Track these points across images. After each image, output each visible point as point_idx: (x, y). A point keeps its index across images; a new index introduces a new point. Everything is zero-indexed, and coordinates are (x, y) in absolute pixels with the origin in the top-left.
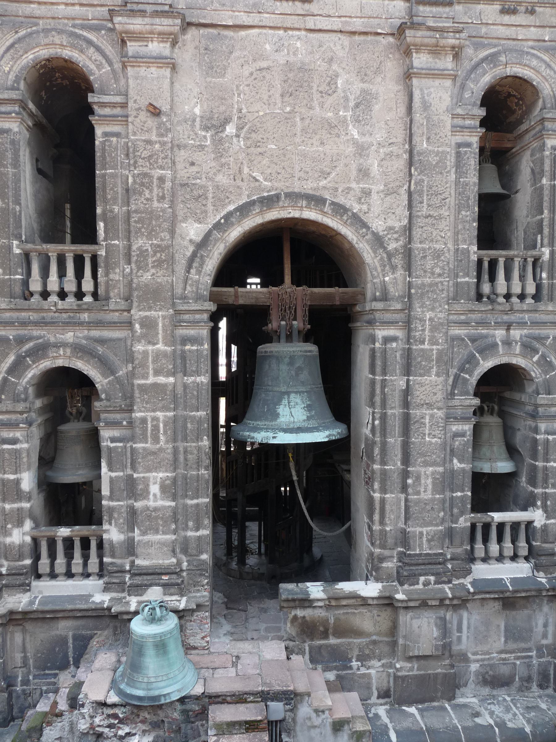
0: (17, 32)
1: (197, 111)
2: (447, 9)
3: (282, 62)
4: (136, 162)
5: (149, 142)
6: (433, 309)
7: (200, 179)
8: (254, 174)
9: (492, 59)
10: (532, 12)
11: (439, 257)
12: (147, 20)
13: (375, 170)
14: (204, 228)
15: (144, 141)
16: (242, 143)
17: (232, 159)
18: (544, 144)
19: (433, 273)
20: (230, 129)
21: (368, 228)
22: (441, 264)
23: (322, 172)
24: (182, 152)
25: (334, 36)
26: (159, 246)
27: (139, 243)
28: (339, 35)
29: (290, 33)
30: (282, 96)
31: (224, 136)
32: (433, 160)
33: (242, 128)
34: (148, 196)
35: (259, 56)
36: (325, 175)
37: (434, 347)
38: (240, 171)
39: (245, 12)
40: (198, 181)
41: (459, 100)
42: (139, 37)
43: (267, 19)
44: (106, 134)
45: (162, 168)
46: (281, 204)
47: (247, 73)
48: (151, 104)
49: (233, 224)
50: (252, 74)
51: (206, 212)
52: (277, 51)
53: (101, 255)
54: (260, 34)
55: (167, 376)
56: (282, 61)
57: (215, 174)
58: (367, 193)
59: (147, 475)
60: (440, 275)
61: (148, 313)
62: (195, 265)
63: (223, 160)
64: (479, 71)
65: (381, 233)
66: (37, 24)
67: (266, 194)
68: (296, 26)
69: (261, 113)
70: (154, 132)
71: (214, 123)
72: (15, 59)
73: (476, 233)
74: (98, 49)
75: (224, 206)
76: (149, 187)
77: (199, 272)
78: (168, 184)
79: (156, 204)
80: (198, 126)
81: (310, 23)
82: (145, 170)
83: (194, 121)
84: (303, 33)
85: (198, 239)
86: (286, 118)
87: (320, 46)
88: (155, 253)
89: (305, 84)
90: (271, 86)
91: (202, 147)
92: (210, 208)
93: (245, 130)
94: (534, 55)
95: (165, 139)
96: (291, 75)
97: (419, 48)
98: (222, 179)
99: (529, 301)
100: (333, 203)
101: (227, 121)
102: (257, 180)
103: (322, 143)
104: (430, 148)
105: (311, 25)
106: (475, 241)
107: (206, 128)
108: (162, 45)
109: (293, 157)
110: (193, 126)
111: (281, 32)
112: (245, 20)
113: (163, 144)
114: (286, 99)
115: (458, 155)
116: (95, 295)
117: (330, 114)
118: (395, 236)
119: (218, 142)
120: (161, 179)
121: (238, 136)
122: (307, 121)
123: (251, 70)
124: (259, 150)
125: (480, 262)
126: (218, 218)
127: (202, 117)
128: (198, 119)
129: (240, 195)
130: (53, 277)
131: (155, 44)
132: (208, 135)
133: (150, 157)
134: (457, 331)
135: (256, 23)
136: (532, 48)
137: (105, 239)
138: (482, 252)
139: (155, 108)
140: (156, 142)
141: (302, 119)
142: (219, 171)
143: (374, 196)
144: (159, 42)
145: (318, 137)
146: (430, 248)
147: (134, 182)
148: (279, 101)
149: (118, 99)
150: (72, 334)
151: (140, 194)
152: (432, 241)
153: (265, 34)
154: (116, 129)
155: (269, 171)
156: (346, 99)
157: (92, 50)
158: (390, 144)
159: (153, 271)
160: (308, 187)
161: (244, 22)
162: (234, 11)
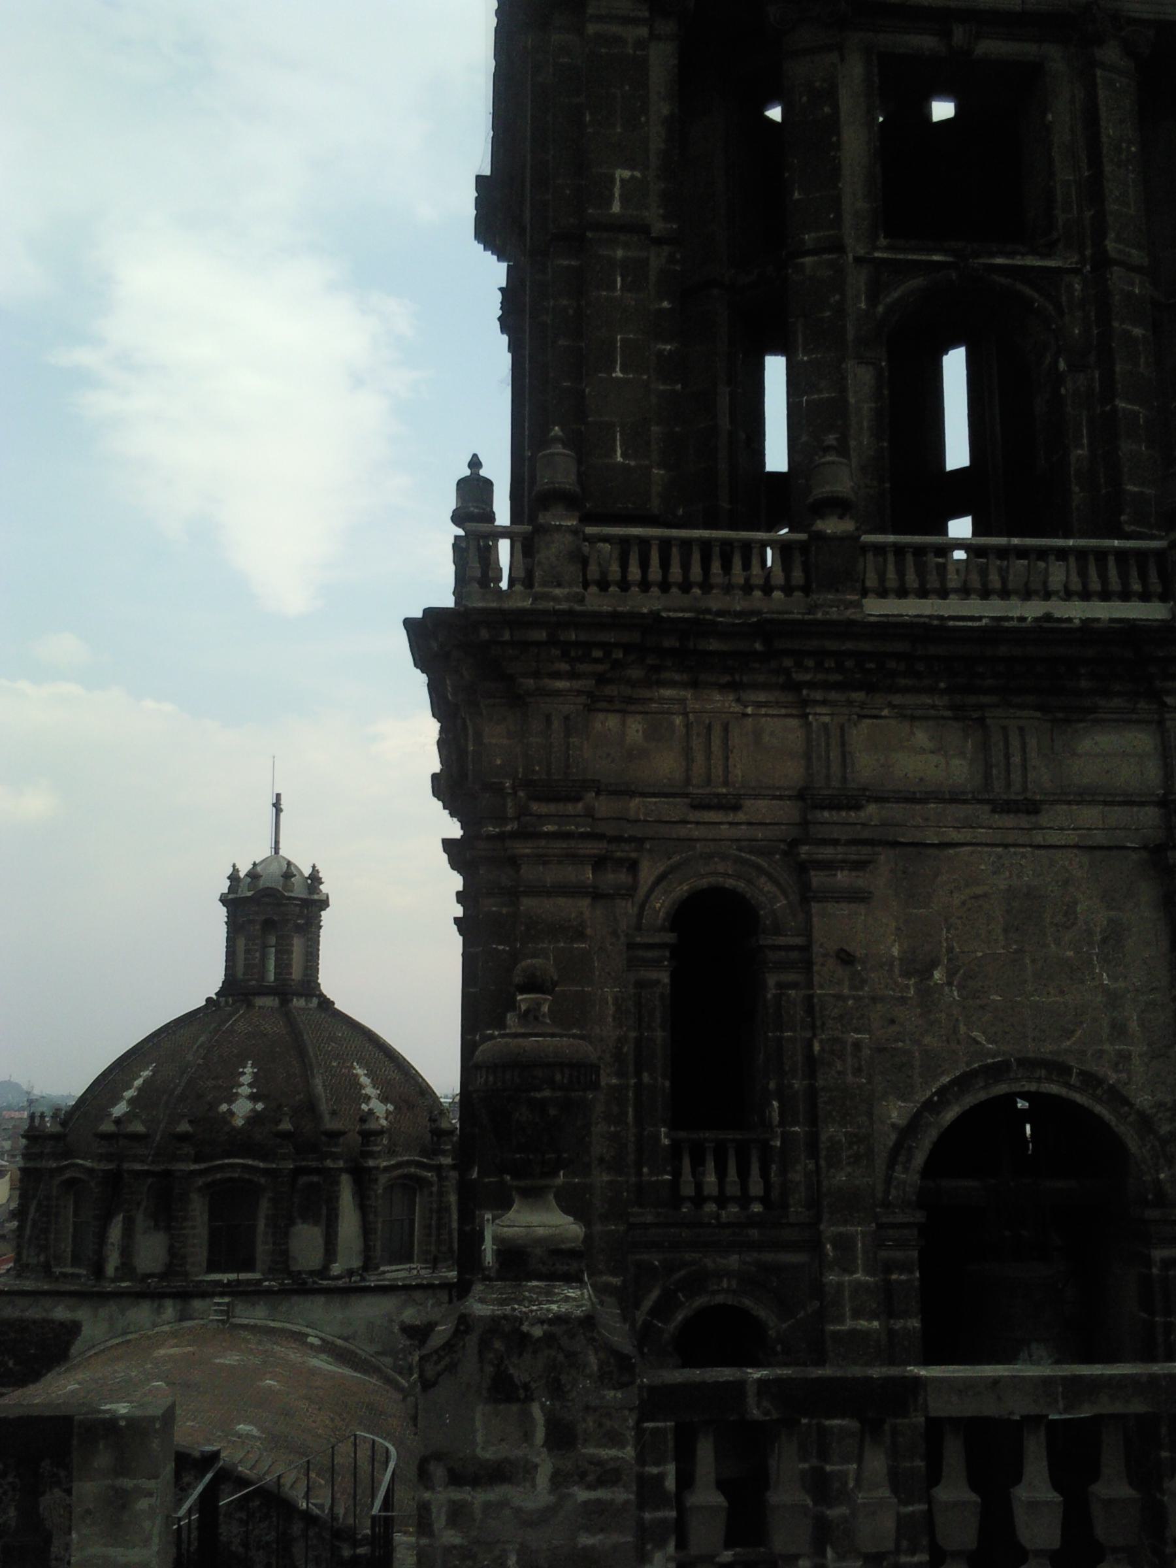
0: (670, 858)
1: (895, 951)
3: (1002, 887)
4: (823, 1024)
5: (839, 997)
12: (840, 849)
13: (1134, 1025)
14: (912, 1107)
15: (834, 996)
16: (955, 993)
17: (943, 1016)
21: (1131, 1105)
24: (879, 1006)
27: (830, 1131)
28: (1075, 851)
29: (1012, 850)
30: (1005, 931)
31: (932, 984)
34: (839, 1068)
36: (1069, 1033)
38: (955, 1030)
39: (954, 827)
40: (900, 1044)
42: (829, 866)
44: (780, 985)
45: (857, 1031)
46: (1012, 1075)
48: (842, 950)
50: (964, 903)
52: (994, 873)
53: (776, 1146)
54: (972, 852)
55: (869, 1320)
58: (1125, 1057)
59: (845, 1467)
61: (842, 1229)
62: (901, 1159)
65: (1149, 1112)
67: (990, 1061)
68: (1020, 841)
69: (979, 954)
74: (770, 877)
77: (906, 1170)
78: (866, 1052)
79: (850, 1079)
80: (897, 971)
81: (1039, 839)
83: (892, 965)
85: (902, 1122)
91: (903, 1000)
95: (861, 993)
100: (1082, 1073)
101: (934, 964)
102: (978, 1043)
103: (1062, 992)
107: (907, 974)
108: (854, 874)
111: (999, 850)
112: (955, 836)
113: (857, 999)
116: (765, 1200)
118: (1168, 1114)
120: (857, 1045)
121: (950, 984)
123: (963, 897)
126: (928, 1094)
127: (901, 959)
128: (897, 963)
132: (912, 982)
135: (969, 838)
137: (782, 1123)
139: (848, 954)
141: (1033, 961)
143: (1136, 1061)
144: (850, 870)
147: (822, 1050)
149: (798, 941)
150: (736, 1257)
153: (980, 852)
154: (791, 977)
157: (763, 879)
158: (1152, 990)
159: (849, 1169)
160: (1048, 1049)
161: (953, 839)
162: (940, 827)
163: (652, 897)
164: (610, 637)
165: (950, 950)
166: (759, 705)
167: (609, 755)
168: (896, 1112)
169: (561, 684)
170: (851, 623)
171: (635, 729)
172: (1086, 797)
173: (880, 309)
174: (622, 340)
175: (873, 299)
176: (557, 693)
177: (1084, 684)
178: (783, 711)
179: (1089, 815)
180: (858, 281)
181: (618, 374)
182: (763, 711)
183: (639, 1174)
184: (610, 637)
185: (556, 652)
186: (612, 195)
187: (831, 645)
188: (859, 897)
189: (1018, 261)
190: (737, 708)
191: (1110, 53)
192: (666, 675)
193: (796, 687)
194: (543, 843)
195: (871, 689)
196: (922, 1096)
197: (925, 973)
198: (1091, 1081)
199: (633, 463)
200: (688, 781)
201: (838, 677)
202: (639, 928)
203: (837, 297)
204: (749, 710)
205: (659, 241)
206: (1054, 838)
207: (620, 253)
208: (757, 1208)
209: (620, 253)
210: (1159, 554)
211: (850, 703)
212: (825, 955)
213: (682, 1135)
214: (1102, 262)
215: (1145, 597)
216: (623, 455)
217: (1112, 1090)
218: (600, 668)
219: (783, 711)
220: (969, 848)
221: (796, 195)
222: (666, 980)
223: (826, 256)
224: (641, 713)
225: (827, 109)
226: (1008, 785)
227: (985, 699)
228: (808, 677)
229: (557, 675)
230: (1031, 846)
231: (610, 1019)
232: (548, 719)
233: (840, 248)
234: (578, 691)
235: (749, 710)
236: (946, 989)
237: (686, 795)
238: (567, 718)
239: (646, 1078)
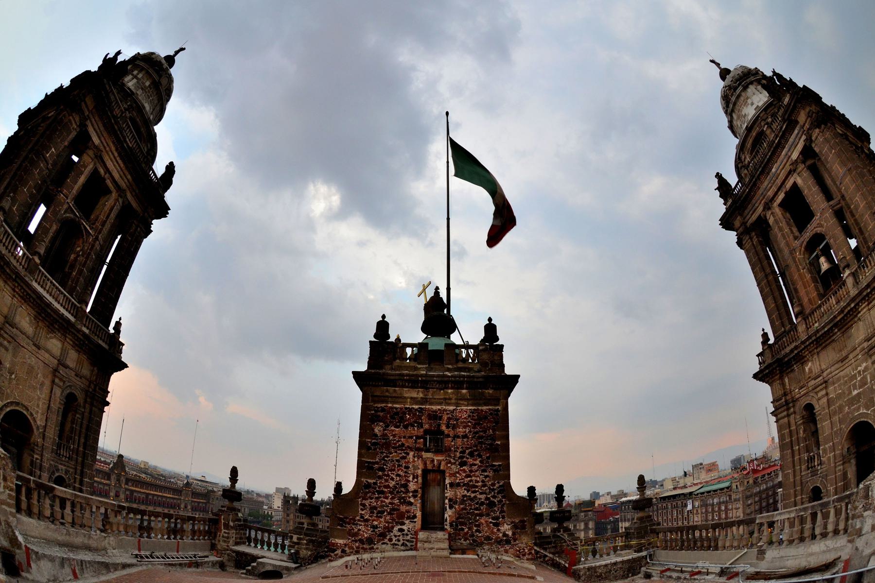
1: (8, 366)
10: (81, 378)
20: (13, 376)
35: (25, 358)
43: (29, 348)
97: (57, 377)
101: (13, 373)
107: (9, 373)
112: (25, 346)
119: (10, 379)
170: (28, 283)
172: (47, 351)
175: (64, 214)
177: (56, 327)
179: (47, 355)
180: (65, 206)
187: (24, 287)
188: (7, 349)
189: (87, 226)
190: (3, 287)
191: (121, 200)
193: (14, 291)
195: (25, 301)
197: (11, 374)
198: (32, 415)
205: (47, 168)
206: (40, 357)
209: (42, 165)
210: (78, 307)
211: (21, 302)
214: (97, 238)
217: (34, 418)
220: (26, 350)
226: (37, 340)
227: (40, 318)
228: (17, 290)
233: (67, 198)
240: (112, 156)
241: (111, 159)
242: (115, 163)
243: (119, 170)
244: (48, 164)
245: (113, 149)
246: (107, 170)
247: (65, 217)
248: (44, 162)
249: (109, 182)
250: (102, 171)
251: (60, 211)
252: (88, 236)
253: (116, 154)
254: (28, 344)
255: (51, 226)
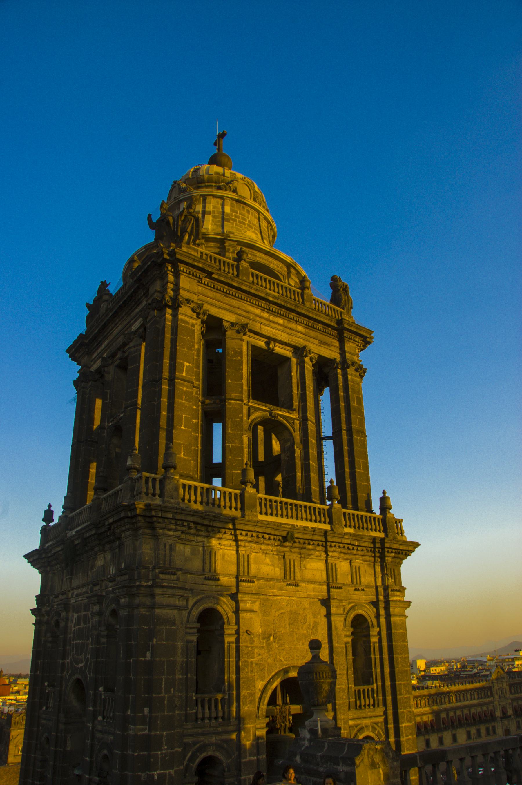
1: (260, 631)
2: (340, 590)
4: (242, 655)
5: (247, 647)
6: (344, 714)
7: (262, 661)
8: (281, 658)
9: (352, 608)
10: (363, 590)
11: (344, 691)
14: (264, 683)
17: (273, 652)
18: (370, 641)
19: (343, 698)
20: (271, 638)
22: (345, 694)
23: (303, 656)
25: (304, 599)
26: (251, 693)
32: (340, 650)
33: (276, 638)
34: (247, 671)
37: (345, 731)
38: (276, 657)
40: (262, 662)
41: (345, 625)
45: (252, 658)
47: (277, 615)
49: (275, 681)
50: (278, 615)
51: (264, 676)
54: (281, 599)
55: (254, 756)
56: (289, 610)
57: (268, 659)
60: (345, 699)
62: (262, 701)
63: (270, 653)
64: (350, 613)
66: (204, 594)
69: (283, 632)
70: (249, 643)
71: (266, 636)
72: (197, 609)
73: (353, 679)
75: (271, 673)
76: (247, 667)
77: (263, 705)
78: (254, 665)
79: (250, 674)
82: (246, 659)
83: (259, 635)
84: (295, 598)
86: (291, 634)
87: (301, 604)
88: (249, 697)
89: (297, 619)
90: (285, 620)
92: (266, 674)
93: (277, 639)
94: (365, 606)
96: (292, 616)
98: (270, 661)
99: (372, 707)
102: (282, 661)
104: (339, 645)
105: (298, 595)
106: (353, 683)
107: (264, 639)
108: (251, 605)
109: (294, 650)
110: (259, 638)
111: (288, 598)
113: (252, 647)
114: (290, 626)
115: (346, 646)
116: (223, 718)
117: (305, 632)
119: (269, 644)
120: (252, 663)
121: (275, 642)
122: (298, 635)
123: (278, 613)
124: (282, 648)
125: (355, 691)
126: (269, 678)
127: (262, 634)
129: (276, 668)
130: (207, 711)
131: (249, 604)
132: (265, 641)
133: (248, 653)
134: (351, 723)
136: (364, 603)
138: (356, 687)
139: (250, 632)
140: (249, 647)
141: (296, 634)
142: (269, 657)
145: (301, 641)
146: (341, 688)
147: (242, 665)
148: (288, 627)
150: (214, 738)
151: (244, 670)
152: (341, 684)
155: (286, 657)
156: (310, 625)
157: (225, 606)
163: (192, 611)
164: (190, 518)
165: (275, 631)
166: (225, 546)
167: (180, 559)
168: (260, 685)
169: (171, 533)
171: (188, 550)
173: (250, 420)
174: (185, 417)
176: (169, 536)
178: (231, 548)
181: (183, 428)
182: (226, 548)
183: (186, 710)
184: (190, 518)
185: (173, 522)
186: (183, 369)
192: (200, 533)
194: (165, 589)
196: (267, 679)
199: (186, 458)
200: (204, 570)
201: (249, 539)
202: (188, 621)
203: (241, 415)
204: (222, 547)
206: (302, 595)
207: (185, 389)
208: (220, 720)
209: (185, 389)
212: (243, 632)
213: (199, 695)
215: (325, 522)
216: (184, 455)
218: (184, 529)
219: (231, 548)
220: (280, 597)
221: (229, 381)
222: (196, 640)
223: (238, 402)
224: (190, 545)
225: (239, 358)
226: (290, 578)
229: (170, 530)
230: (296, 597)
231: (180, 654)
232: (165, 545)
233: (242, 401)
234: (176, 536)
235: (222, 547)
236: (274, 644)
237: (204, 575)
238: (171, 545)
239: (189, 675)
240: (263, 321)
241: (265, 325)
242: (272, 325)
243: (282, 328)
244: (193, 383)
245: (258, 311)
246: (269, 339)
247: (252, 422)
248: (186, 383)
249: (279, 349)
250: (261, 343)
251: (242, 419)
252: (293, 423)
253: (266, 315)
254: (281, 589)
255: (242, 442)
